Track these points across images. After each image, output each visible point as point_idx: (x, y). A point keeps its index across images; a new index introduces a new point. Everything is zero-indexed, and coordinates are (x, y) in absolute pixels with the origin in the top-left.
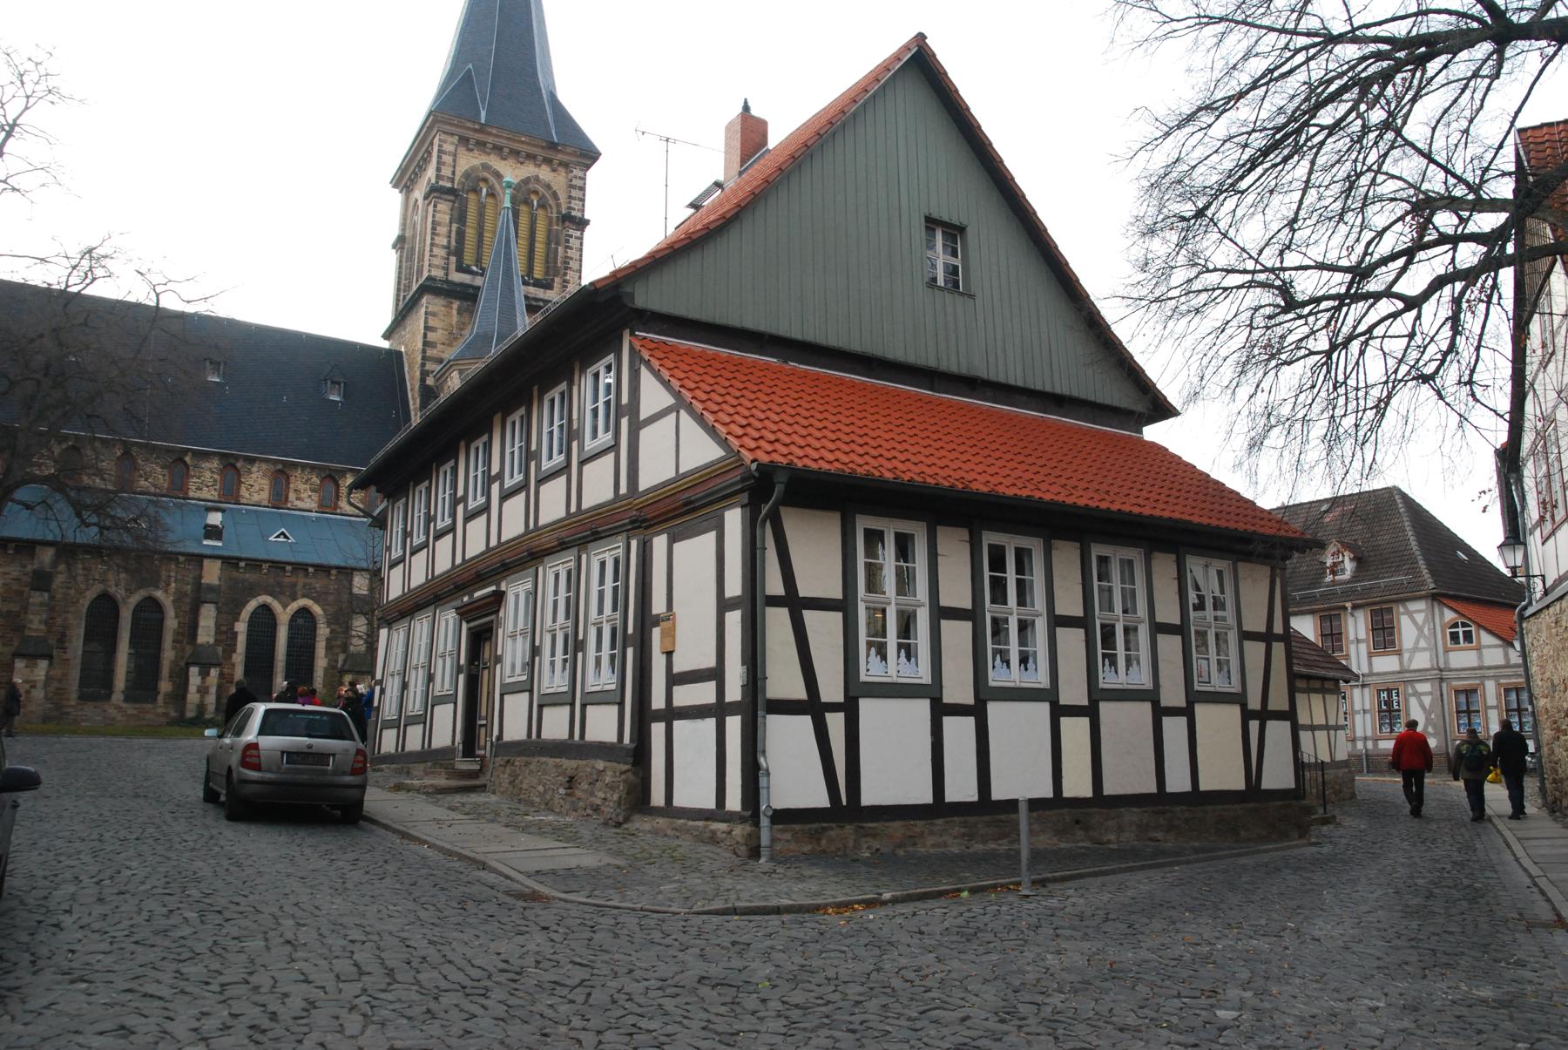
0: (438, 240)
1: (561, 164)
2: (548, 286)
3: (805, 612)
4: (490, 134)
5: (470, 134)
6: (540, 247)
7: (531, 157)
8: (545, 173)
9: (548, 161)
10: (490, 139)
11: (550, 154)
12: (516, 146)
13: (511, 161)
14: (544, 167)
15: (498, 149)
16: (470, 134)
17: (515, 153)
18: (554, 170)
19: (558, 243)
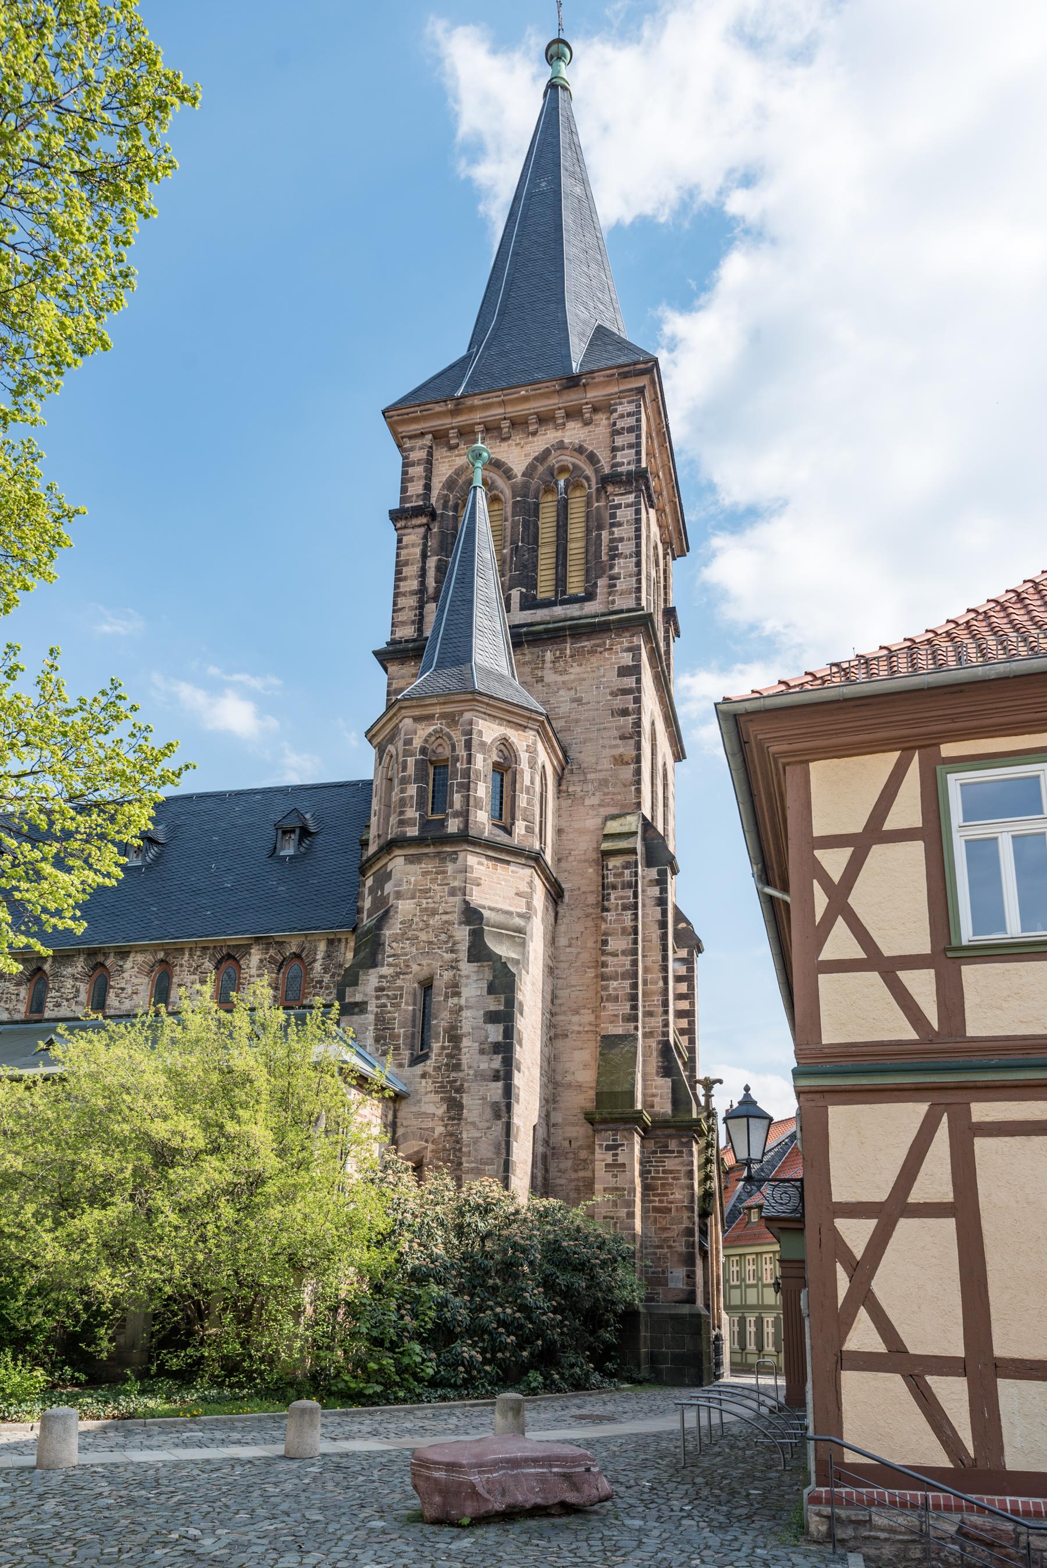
0: (405, 586)
1: (595, 410)
2: (590, 596)
3: (910, 1200)
4: (472, 409)
5: (446, 422)
6: (576, 547)
7: (545, 419)
8: (573, 433)
9: (573, 414)
10: (477, 417)
11: (572, 398)
12: (513, 410)
13: (517, 438)
14: (571, 425)
15: (491, 429)
16: (446, 422)
17: (518, 424)
18: (587, 423)
19: (600, 527)
